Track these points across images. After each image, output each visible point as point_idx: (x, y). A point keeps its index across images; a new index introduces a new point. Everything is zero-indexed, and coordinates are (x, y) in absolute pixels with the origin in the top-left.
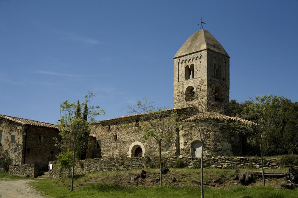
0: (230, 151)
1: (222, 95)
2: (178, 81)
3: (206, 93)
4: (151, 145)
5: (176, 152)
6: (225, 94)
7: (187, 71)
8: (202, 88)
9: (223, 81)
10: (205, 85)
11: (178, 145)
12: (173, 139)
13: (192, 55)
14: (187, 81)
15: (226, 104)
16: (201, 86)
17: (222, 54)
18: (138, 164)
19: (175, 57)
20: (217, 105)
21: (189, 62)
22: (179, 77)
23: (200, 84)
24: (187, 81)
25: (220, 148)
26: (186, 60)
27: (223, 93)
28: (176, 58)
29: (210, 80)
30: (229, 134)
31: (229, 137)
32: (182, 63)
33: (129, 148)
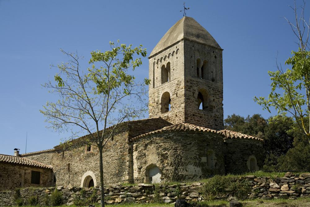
1: (210, 102)
2: (154, 87)
3: (183, 99)
6: (216, 100)
7: (164, 73)
8: (179, 92)
9: (211, 82)
10: (182, 89)
11: (131, 173)
13: (168, 50)
14: (162, 86)
15: (217, 114)
17: (209, 46)
18: (4, 202)
19: (150, 56)
20: (202, 115)
22: (155, 81)
23: (176, 87)
24: (162, 86)
25: (183, 175)
26: (162, 58)
27: (212, 99)
28: (152, 57)
29: (189, 80)
30: (197, 153)
31: (198, 157)
32: (157, 63)
33: (81, 180)
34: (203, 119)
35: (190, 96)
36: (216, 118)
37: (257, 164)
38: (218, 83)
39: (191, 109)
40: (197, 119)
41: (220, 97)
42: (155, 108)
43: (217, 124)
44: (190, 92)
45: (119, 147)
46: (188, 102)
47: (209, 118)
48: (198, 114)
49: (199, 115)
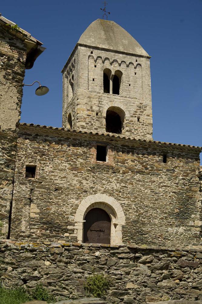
4: (141, 207)
5: (200, 231)
12: (194, 204)
13: (121, 55)
16: (139, 114)
21: (111, 64)
23: (138, 109)
26: (107, 59)
32: (96, 61)
33: (77, 206)
42: (94, 120)
45: (181, 177)
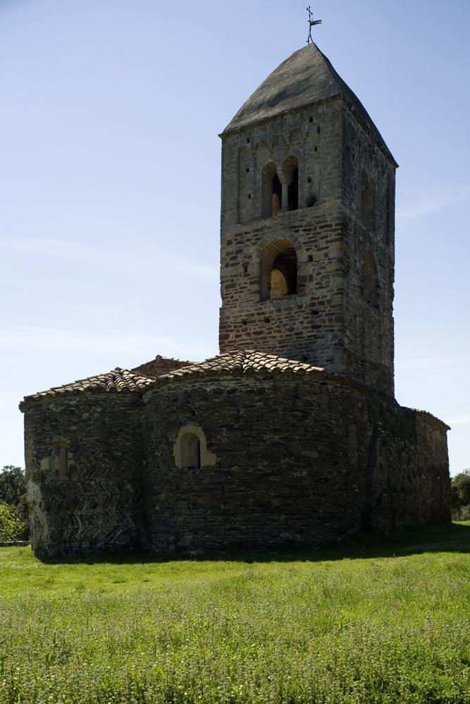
0: (40, 507)
6: (317, 255)
15: (319, 293)
20: (270, 313)
34: (273, 324)
35: (236, 276)
36: (315, 308)
37: (209, 446)
38: (324, 202)
39: (236, 309)
40: (253, 331)
41: (331, 241)
43: (319, 324)
44: (234, 268)
46: (229, 296)
47: (293, 314)
48: (259, 314)
49: (262, 317)
